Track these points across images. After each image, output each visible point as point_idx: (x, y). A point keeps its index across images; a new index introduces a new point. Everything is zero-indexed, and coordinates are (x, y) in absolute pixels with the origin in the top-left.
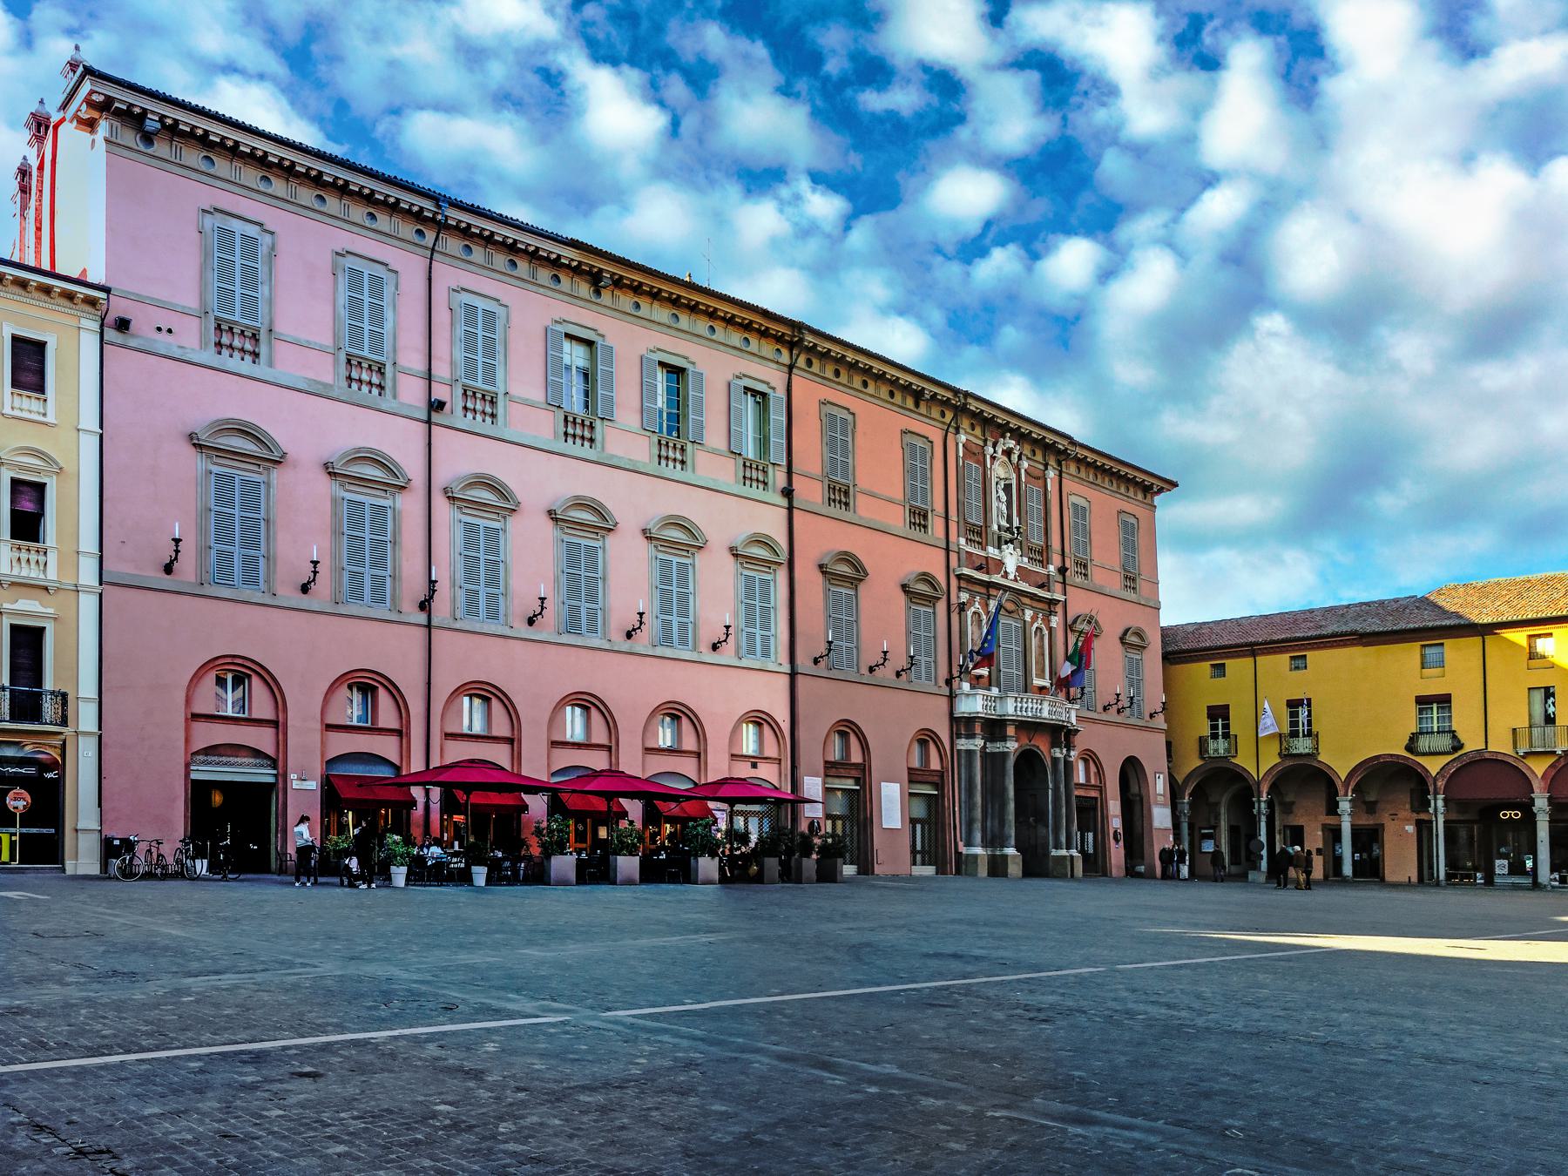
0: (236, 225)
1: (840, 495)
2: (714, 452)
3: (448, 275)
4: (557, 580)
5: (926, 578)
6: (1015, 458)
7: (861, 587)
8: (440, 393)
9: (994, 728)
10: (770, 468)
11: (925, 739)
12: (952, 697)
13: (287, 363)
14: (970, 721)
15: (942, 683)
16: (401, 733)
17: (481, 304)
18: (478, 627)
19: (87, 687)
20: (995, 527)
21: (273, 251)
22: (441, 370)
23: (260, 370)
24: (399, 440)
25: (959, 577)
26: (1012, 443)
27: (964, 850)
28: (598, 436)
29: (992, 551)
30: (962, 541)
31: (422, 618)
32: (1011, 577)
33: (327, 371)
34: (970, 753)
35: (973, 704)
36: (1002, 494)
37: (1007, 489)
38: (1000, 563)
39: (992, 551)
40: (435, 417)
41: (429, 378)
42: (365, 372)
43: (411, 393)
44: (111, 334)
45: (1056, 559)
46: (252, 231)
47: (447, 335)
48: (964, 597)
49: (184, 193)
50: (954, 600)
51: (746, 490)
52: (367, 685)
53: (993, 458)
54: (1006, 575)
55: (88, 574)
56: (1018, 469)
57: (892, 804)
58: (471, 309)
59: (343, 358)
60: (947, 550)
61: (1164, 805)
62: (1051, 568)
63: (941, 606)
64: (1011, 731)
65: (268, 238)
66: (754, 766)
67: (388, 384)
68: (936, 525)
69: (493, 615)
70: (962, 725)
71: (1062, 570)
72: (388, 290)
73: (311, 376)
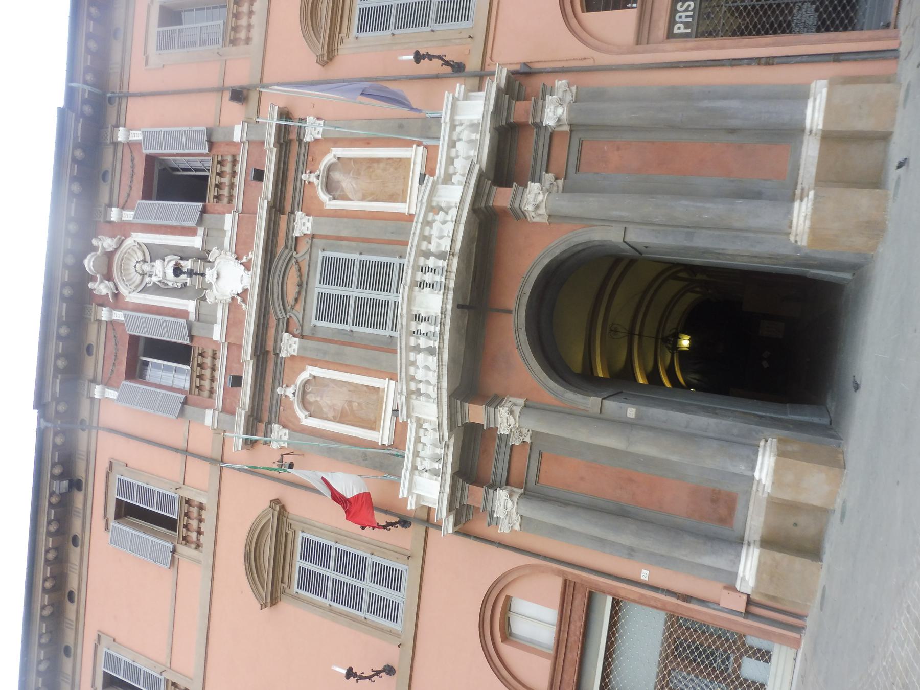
5: (252, 557)
6: (108, 243)
11: (495, 622)
12: (427, 520)
14: (461, 512)
20: (190, 306)
29: (217, 333)
35: (426, 486)
38: (232, 305)
48: (280, 435)
56: (122, 230)
64: (476, 413)
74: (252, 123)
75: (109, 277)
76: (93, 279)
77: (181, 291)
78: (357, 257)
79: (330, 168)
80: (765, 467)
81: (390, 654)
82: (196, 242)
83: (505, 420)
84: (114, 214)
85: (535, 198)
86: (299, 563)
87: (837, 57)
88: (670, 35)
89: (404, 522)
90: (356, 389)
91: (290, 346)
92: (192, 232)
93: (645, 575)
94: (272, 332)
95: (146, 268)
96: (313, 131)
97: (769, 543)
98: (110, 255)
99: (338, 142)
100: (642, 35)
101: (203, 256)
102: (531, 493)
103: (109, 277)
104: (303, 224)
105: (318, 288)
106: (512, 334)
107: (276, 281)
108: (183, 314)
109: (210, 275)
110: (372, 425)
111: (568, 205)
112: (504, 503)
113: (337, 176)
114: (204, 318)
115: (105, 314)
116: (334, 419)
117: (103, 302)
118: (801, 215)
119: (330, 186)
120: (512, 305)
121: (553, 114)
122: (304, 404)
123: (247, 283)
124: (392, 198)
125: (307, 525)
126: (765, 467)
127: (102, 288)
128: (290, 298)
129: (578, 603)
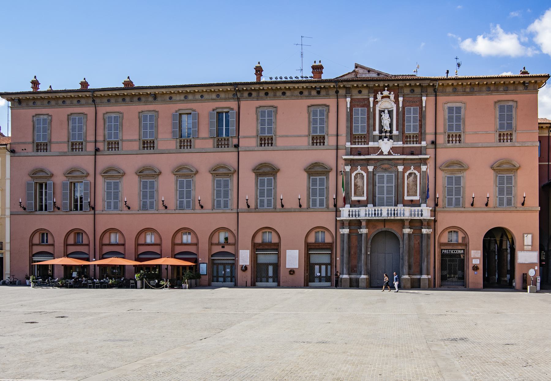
0: (42, 117)
1: (266, 141)
2: (203, 138)
3: (102, 110)
4: (139, 194)
5: (316, 164)
7: (278, 174)
8: (100, 146)
9: (355, 224)
10: (230, 139)
12: (337, 212)
13: (55, 148)
14: (342, 222)
15: (331, 206)
16: (88, 245)
17: (113, 115)
18: (110, 212)
19: (8, 240)
20: (377, 133)
21: (51, 121)
22: (100, 138)
23: (48, 153)
24: (84, 162)
25: (345, 160)
26: (386, 93)
27: (341, 276)
28: (155, 145)
29: (371, 144)
30: (348, 145)
31: (92, 212)
32: (385, 153)
33: (65, 148)
34: (344, 234)
35: (345, 212)
36: (386, 116)
37: (390, 112)
39: (371, 144)
40: (97, 153)
41: (96, 141)
42: (76, 147)
43: (90, 148)
44: (12, 154)
45: (430, 138)
46: (45, 117)
47: (102, 127)
48: (348, 168)
49: (28, 112)
50: (341, 168)
51: (220, 149)
52: (78, 233)
53: (375, 103)
54: (382, 153)
55: (8, 212)
56: (397, 102)
57: (293, 259)
58: (110, 118)
59: (70, 143)
60: (337, 149)
61: (532, 250)
62: (424, 144)
63: (332, 175)
65: (50, 118)
66: (223, 247)
67: (84, 147)
68: (331, 141)
69: (116, 208)
70: (343, 224)
71: (434, 143)
72: (84, 121)
73: (61, 151)
74: (426, 148)
75: (383, 98)
76: (382, 94)
77: (381, 132)
78: (394, 185)
79: (415, 174)
80: (363, 276)
81: (304, 205)
82: (395, 132)
83: (364, 231)
84: (401, 99)
85: (407, 231)
86: (318, 178)
87: (435, 279)
88: (442, 250)
89: (335, 205)
90: (363, 188)
91: (371, 168)
92: (397, 130)
93: (338, 259)
94: (373, 162)
95: (386, 111)
96: (424, 168)
97: (350, 279)
98: (389, 97)
99: (420, 174)
100: (441, 244)
101: (391, 138)
102: (349, 235)
103: (383, 98)
104: (401, 168)
105: (385, 175)
106: (381, 228)
107: (386, 162)
108: (375, 130)
109: (386, 140)
110: (355, 194)
111: (406, 237)
112: (346, 231)
113: (413, 175)
114: (374, 140)
115: (371, 100)
116: (355, 183)
117: (375, 98)
118: (407, 277)
119: (410, 174)
120: (386, 227)
121: (424, 231)
122: (357, 174)
123: (385, 153)
124: (408, 192)
125: (328, 178)
126: (363, 276)
127: (379, 96)
128: (383, 166)
129: (329, 247)
